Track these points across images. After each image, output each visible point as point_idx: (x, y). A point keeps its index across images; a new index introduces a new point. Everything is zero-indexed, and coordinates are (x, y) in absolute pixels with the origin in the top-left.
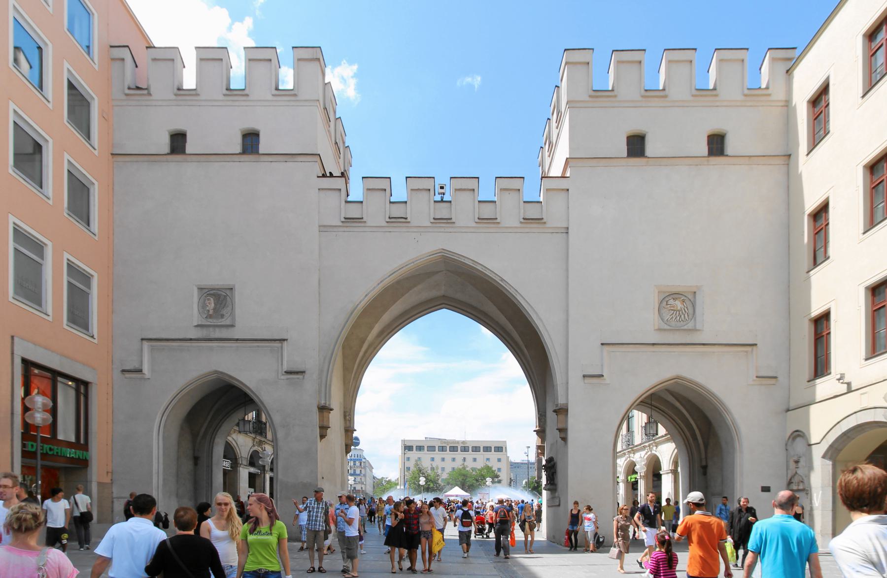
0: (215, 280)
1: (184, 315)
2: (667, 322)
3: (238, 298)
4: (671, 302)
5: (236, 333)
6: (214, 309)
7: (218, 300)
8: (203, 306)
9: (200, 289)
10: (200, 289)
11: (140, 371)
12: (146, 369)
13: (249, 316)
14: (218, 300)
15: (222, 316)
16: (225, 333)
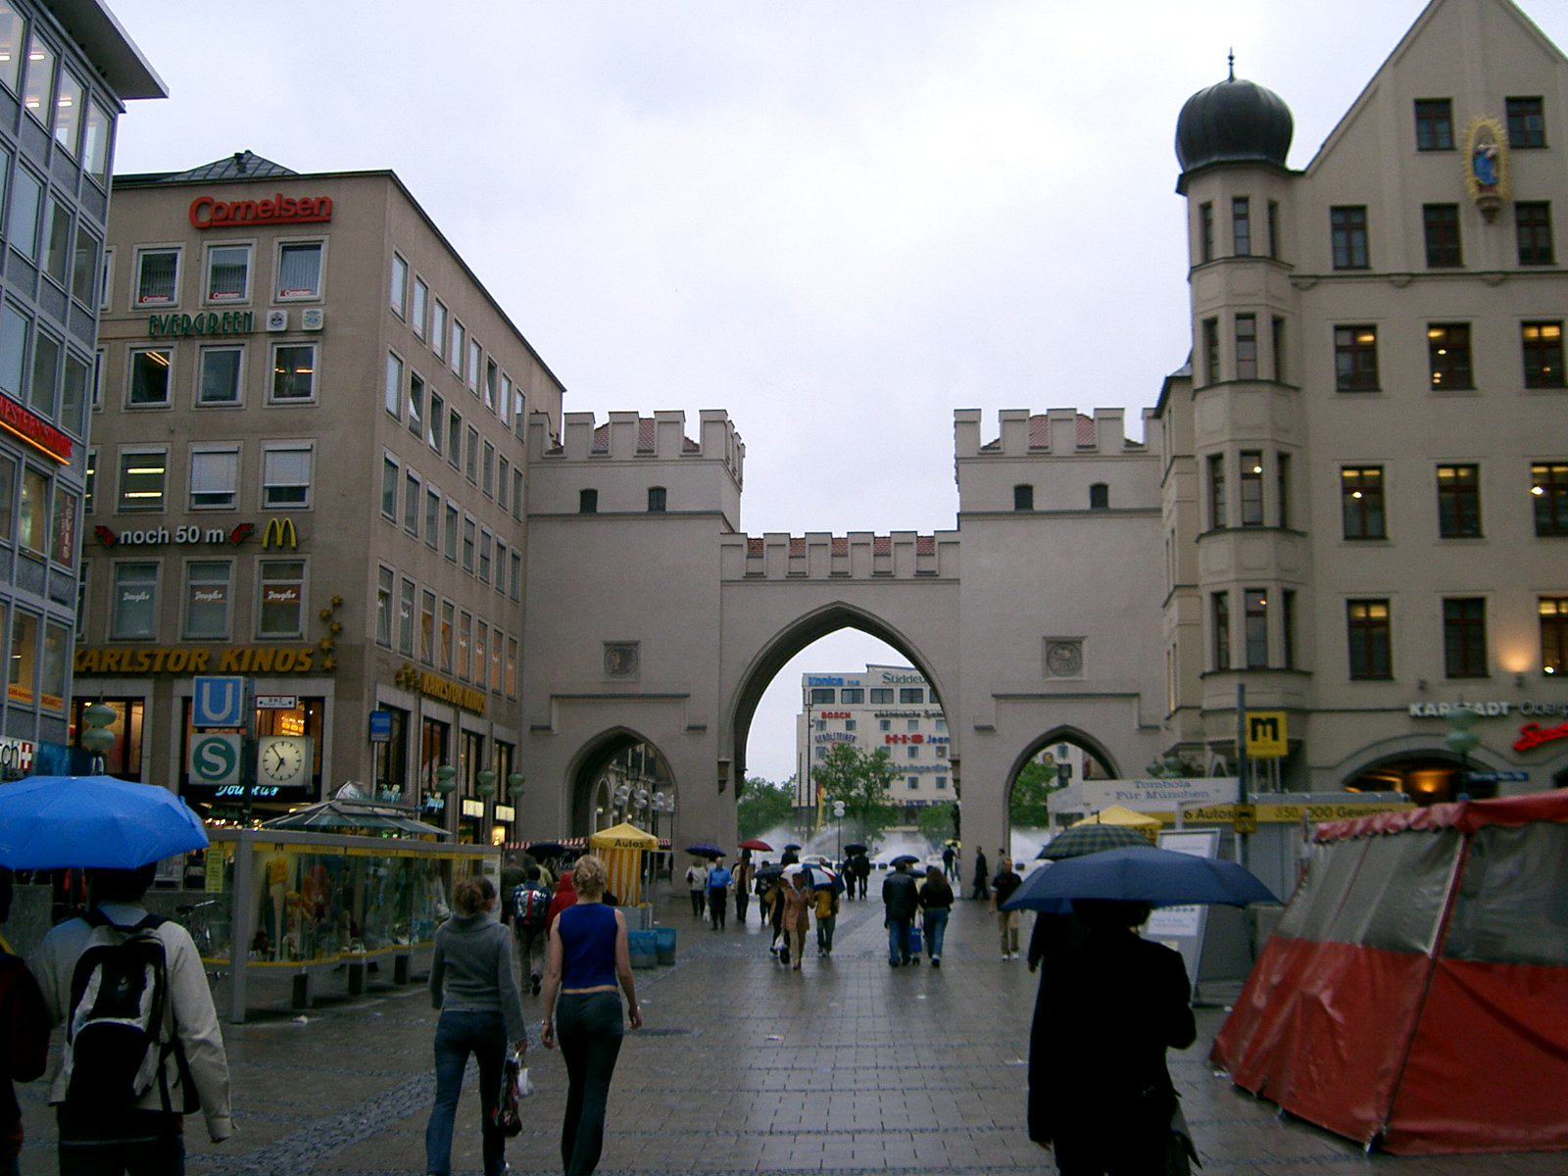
0: (620, 636)
1: (588, 671)
2: (1057, 672)
3: (643, 652)
4: (1060, 651)
5: (641, 691)
6: (620, 664)
7: (623, 655)
8: (608, 662)
9: (607, 644)
10: (607, 644)
11: (549, 728)
12: (554, 727)
13: (654, 671)
14: (623, 655)
15: (628, 671)
16: (630, 690)
